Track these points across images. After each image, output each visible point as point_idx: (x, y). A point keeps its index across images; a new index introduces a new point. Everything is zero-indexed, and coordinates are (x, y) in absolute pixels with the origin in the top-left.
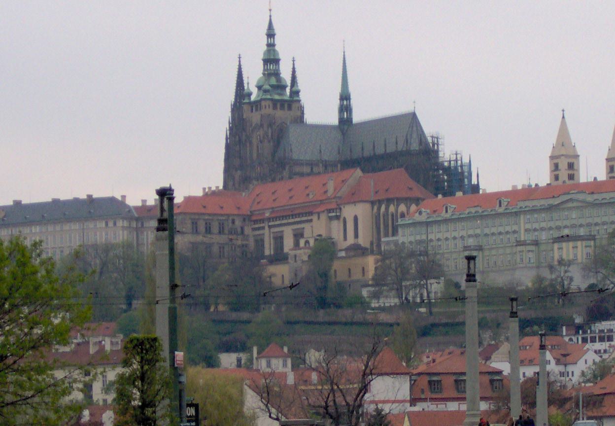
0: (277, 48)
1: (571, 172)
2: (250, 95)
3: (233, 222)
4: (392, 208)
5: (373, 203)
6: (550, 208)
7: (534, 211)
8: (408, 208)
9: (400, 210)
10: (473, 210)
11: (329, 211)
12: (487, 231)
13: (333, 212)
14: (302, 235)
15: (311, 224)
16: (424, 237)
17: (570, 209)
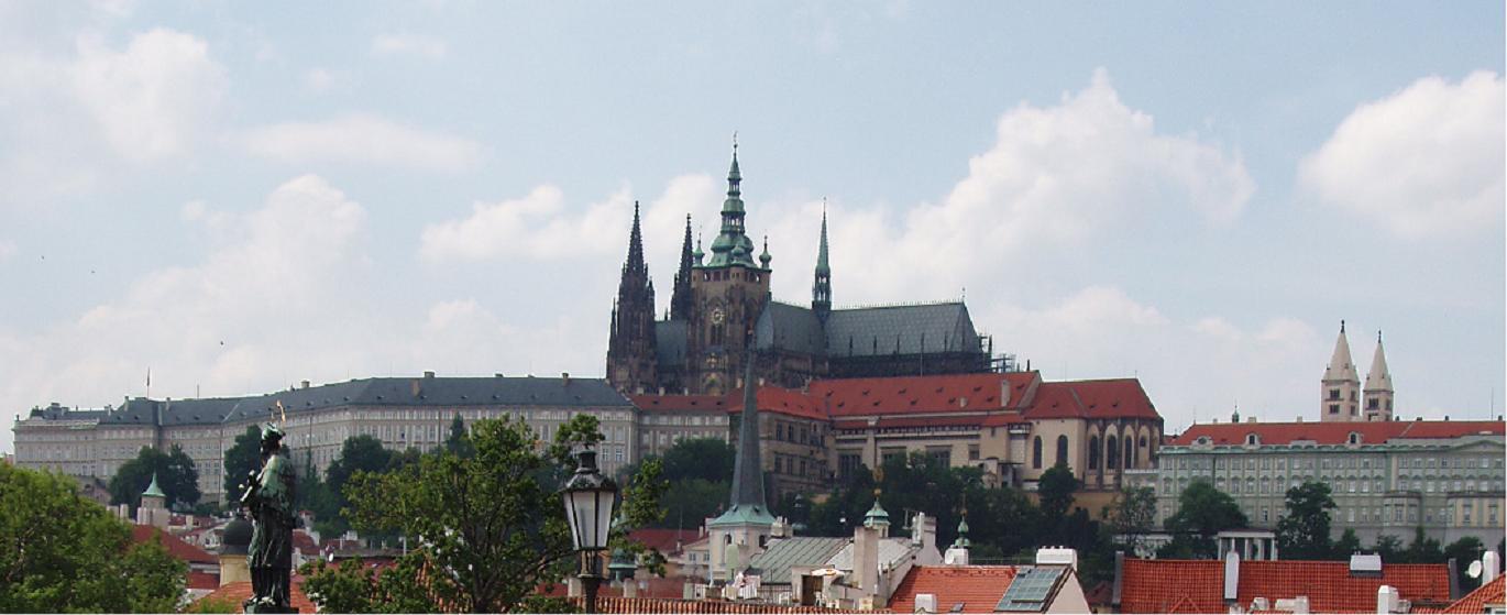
0: (741, 198)
1: (1351, 404)
2: (700, 256)
3: (815, 426)
4: (1129, 431)
5: (1088, 421)
6: (1445, 451)
7: (1416, 451)
8: (1152, 432)
9: (1140, 437)
10: (1303, 444)
11: (1010, 426)
12: (1323, 473)
13: (1019, 428)
14: (946, 454)
15: (974, 442)
16: (1209, 474)
17: (1479, 454)
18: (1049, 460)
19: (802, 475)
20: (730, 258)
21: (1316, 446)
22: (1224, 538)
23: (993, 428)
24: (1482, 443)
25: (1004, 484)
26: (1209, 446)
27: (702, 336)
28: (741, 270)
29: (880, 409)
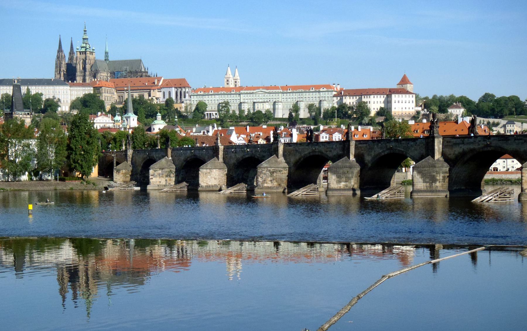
5: (175, 88)
6: (253, 93)
10: (222, 92)
16: (202, 99)
18: (167, 97)
19: (110, 101)
20: (86, 50)
21: (225, 93)
22: (208, 114)
23: (154, 90)
24: (261, 91)
25: (157, 102)
26: (202, 93)
27: (80, 67)
28: (89, 52)
29: (126, 86)
